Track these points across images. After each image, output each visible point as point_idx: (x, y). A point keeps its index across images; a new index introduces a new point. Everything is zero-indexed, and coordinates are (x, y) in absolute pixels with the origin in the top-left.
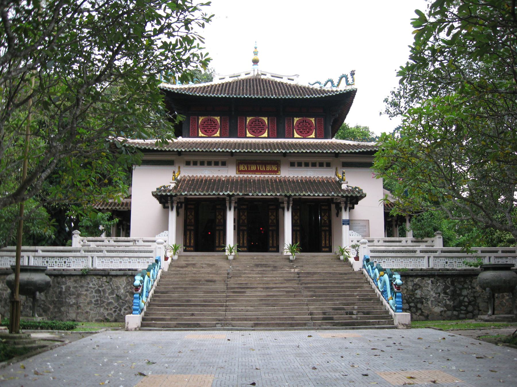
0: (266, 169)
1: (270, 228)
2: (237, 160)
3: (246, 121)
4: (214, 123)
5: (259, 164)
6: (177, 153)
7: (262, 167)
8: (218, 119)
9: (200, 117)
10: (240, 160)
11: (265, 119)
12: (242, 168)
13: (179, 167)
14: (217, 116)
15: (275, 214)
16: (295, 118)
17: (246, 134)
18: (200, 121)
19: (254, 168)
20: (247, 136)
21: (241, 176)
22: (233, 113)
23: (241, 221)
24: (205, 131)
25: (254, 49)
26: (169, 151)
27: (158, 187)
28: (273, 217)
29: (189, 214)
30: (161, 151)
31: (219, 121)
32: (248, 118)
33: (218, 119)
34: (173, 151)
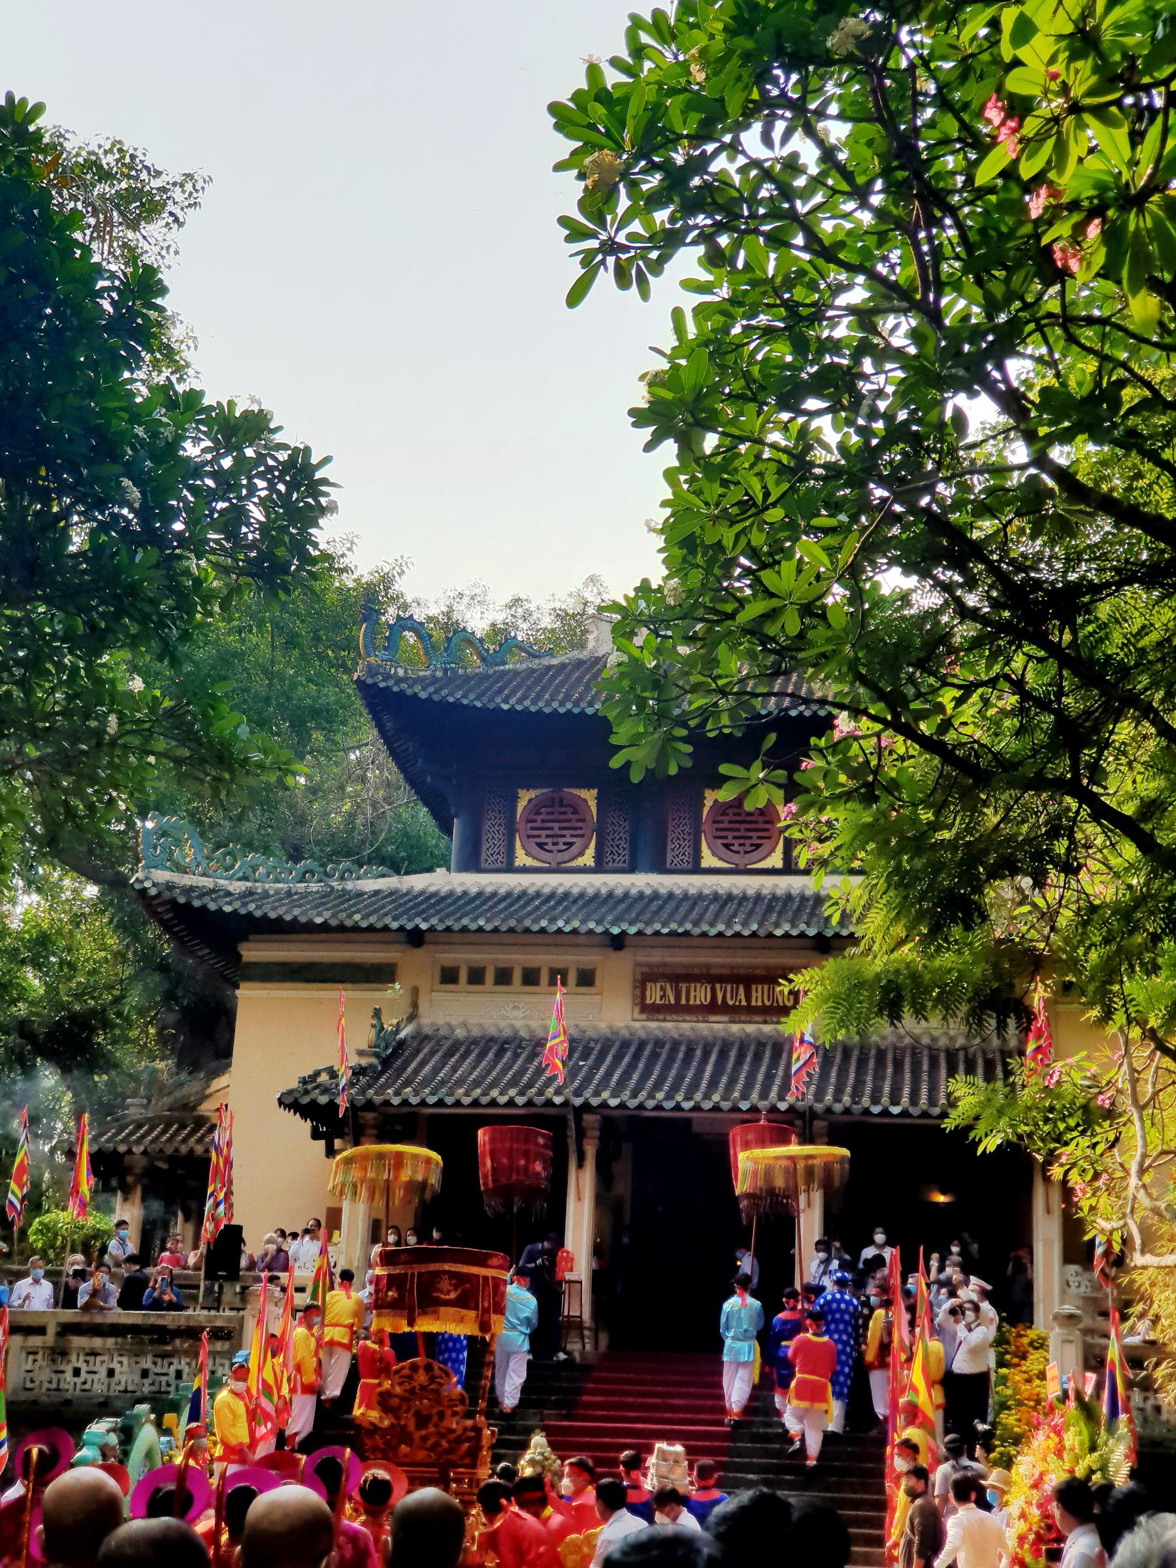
0: (748, 998)
2: (637, 964)
4: (575, 812)
5: (722, 979)
6: (402, 937)
7: (734, 995)
8: (590, 796)
10: (649, 965)
12: (654, 994)
13: (415, 992)
14: (588, 786)
17: (697, 856)
18: (521, 805)
19: (700, 994)
20: (705, 864)
21: (653, 1025)
24: (541, 846)
26: (371, 929)
27: (307, 1072)
30: (342, 928)
31: (593, 804)
33: (590, 796)
34: (386, 929)
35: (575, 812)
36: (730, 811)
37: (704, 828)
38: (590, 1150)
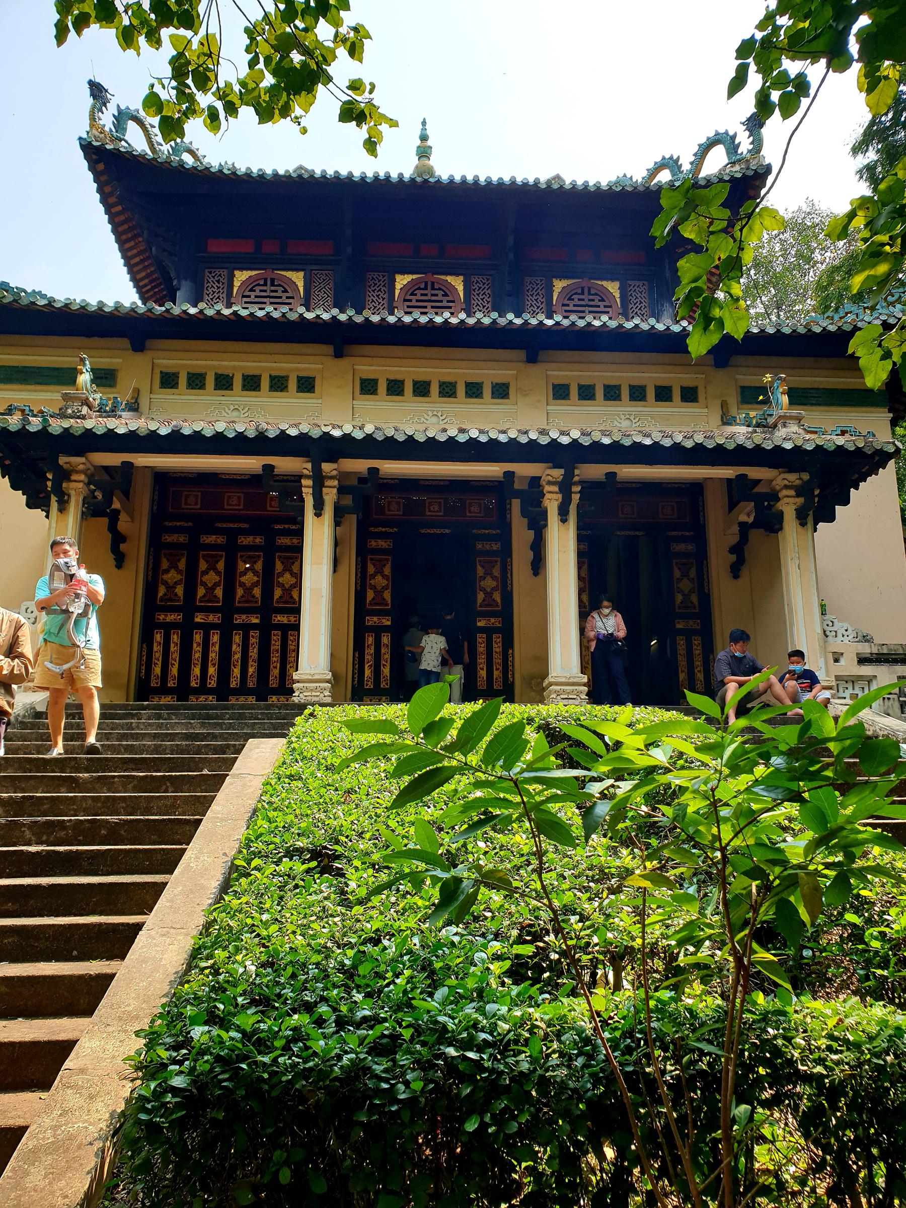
1: (481, 624)
9: (237, 273)
15: (496, 572)
23: (370, 595)
25: (418, 142)
28: (489, 583)
29: (165, 564)
37: (395, 304)
38: (330, 496)
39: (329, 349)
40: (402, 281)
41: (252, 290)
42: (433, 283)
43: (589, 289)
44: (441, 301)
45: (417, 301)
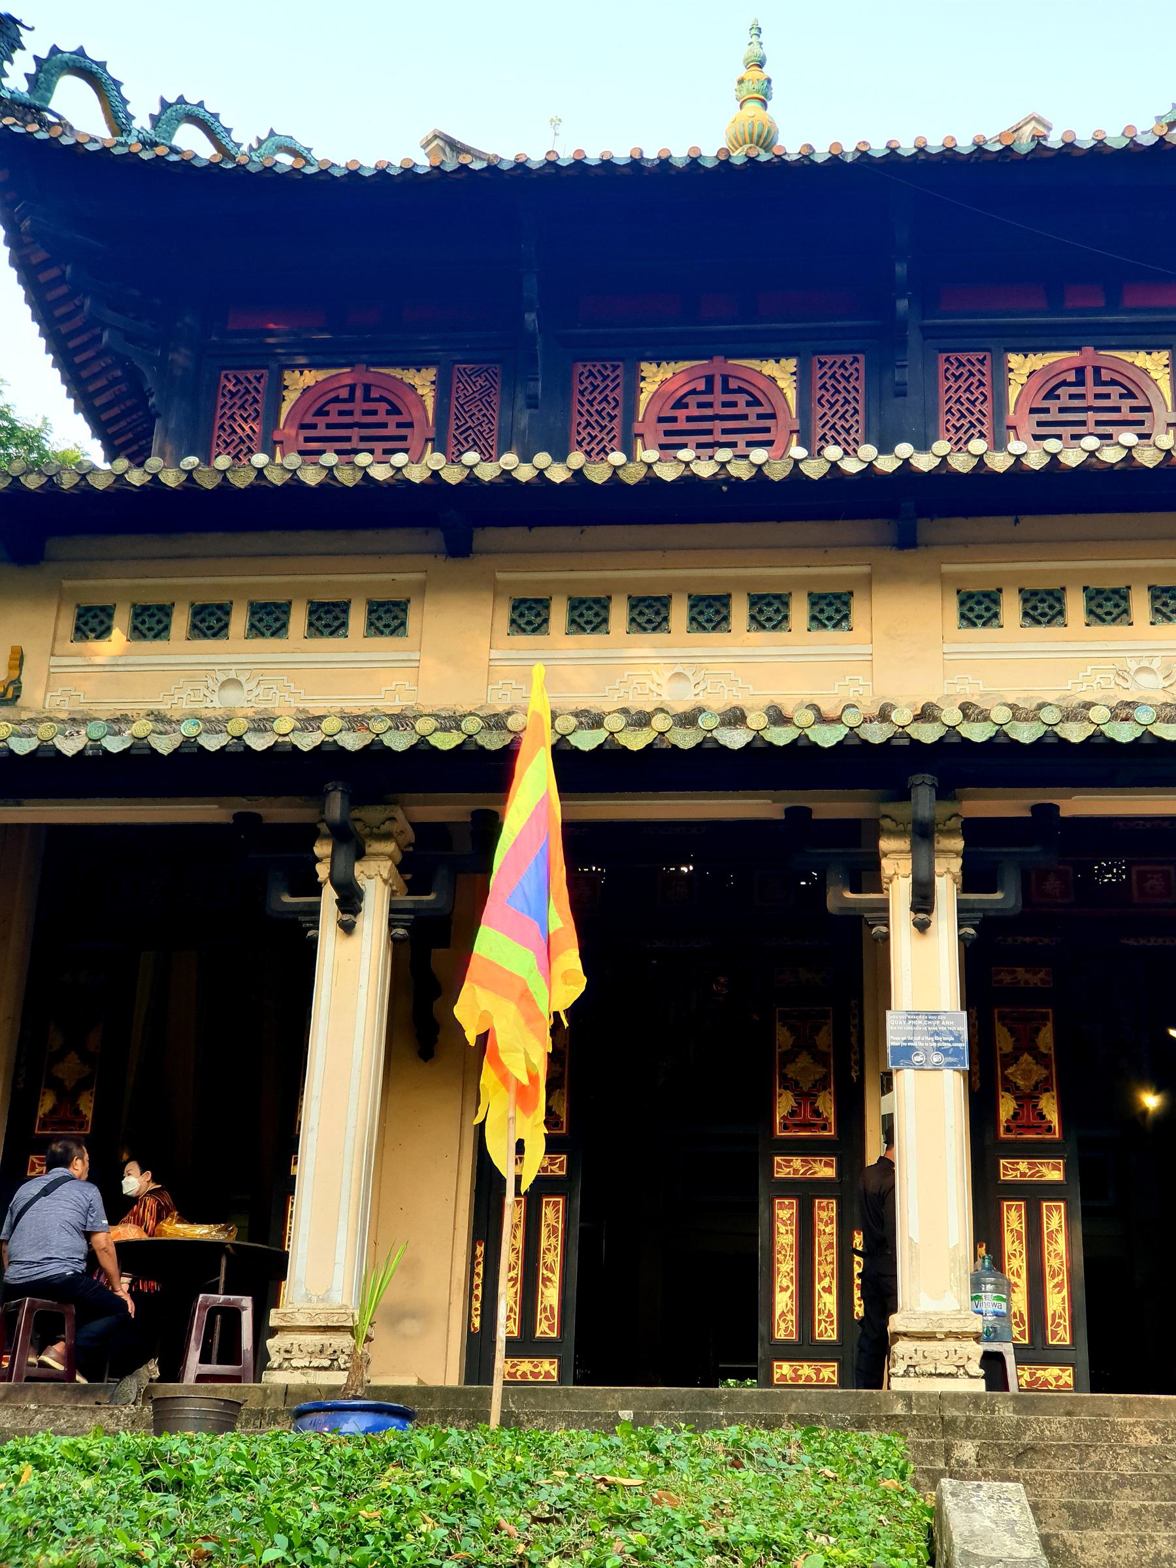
3: (633, 392)
4: (394, 410)
8: (423, 382)
11: (782, 374)
14: (419, 365)
16: (1014, 360)
22: (530, 317)
32: (647, 368)
33: (423, 382)
35: (394, 410)
36: (692, 400)
37: (637, 428)
39: (436, 537)
40: (655, 379)
41: (321, 412)
42: (725, 379)
43: (1097, 370)
44: (745, 417)
45: (690, 419)
